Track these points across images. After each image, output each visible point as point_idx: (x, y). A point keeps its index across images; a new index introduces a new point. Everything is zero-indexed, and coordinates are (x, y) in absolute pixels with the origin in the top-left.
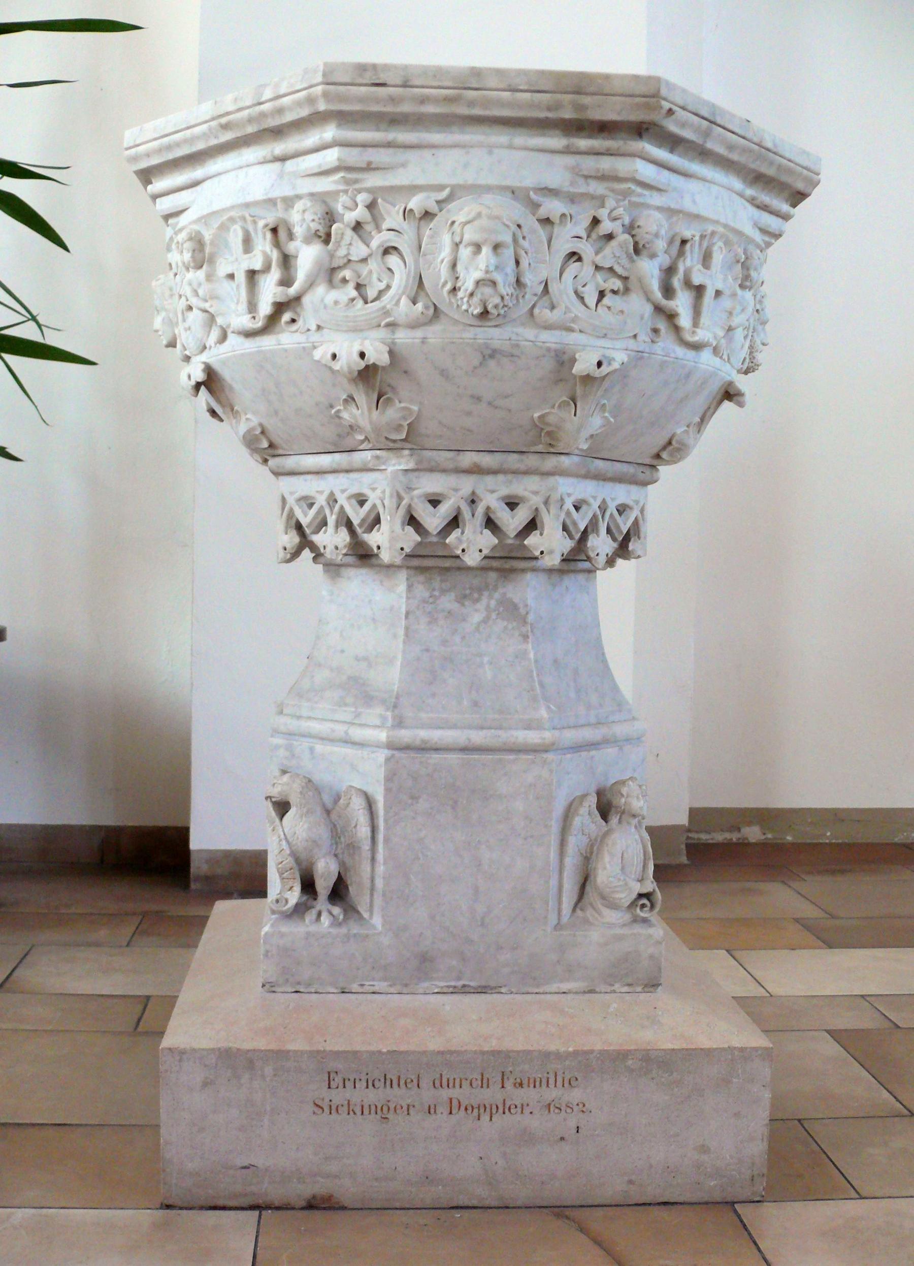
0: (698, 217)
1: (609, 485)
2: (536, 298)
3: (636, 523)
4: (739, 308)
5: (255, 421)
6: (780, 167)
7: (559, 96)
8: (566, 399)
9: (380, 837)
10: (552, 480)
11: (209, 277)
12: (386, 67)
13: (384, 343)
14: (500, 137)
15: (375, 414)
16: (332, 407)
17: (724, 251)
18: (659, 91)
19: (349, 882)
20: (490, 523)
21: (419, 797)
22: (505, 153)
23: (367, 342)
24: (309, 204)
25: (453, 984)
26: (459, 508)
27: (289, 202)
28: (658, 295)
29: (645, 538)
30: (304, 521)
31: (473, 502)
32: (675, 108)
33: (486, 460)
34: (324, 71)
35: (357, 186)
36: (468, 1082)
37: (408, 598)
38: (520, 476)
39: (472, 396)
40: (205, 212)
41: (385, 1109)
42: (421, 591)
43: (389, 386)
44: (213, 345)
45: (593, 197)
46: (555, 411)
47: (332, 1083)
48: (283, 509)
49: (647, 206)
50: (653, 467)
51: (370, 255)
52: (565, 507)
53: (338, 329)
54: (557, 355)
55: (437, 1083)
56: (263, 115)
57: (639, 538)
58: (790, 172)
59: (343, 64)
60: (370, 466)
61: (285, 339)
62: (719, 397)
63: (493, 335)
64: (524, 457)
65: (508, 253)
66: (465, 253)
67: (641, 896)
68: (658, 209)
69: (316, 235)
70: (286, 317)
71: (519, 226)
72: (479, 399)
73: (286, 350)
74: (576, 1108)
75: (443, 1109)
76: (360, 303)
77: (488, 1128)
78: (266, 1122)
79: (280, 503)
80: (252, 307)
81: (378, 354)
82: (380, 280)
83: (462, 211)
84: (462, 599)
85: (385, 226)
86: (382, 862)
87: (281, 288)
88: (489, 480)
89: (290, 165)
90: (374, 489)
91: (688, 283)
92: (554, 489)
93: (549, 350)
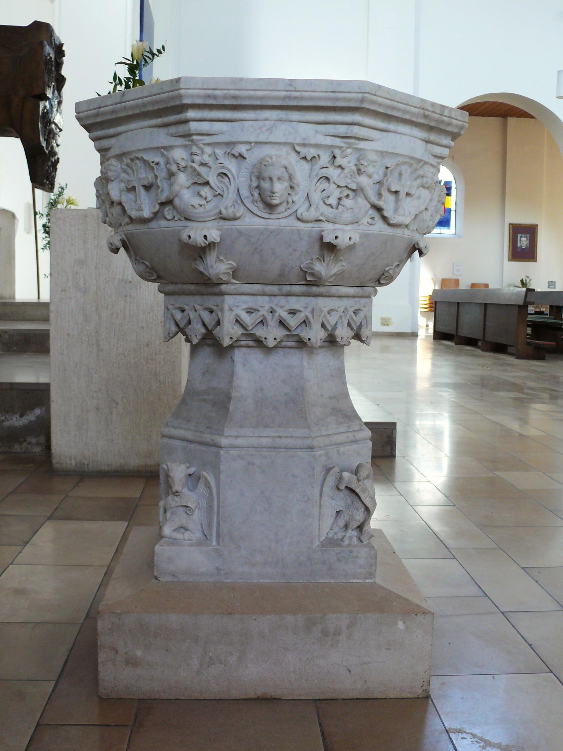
89: (429, 145)
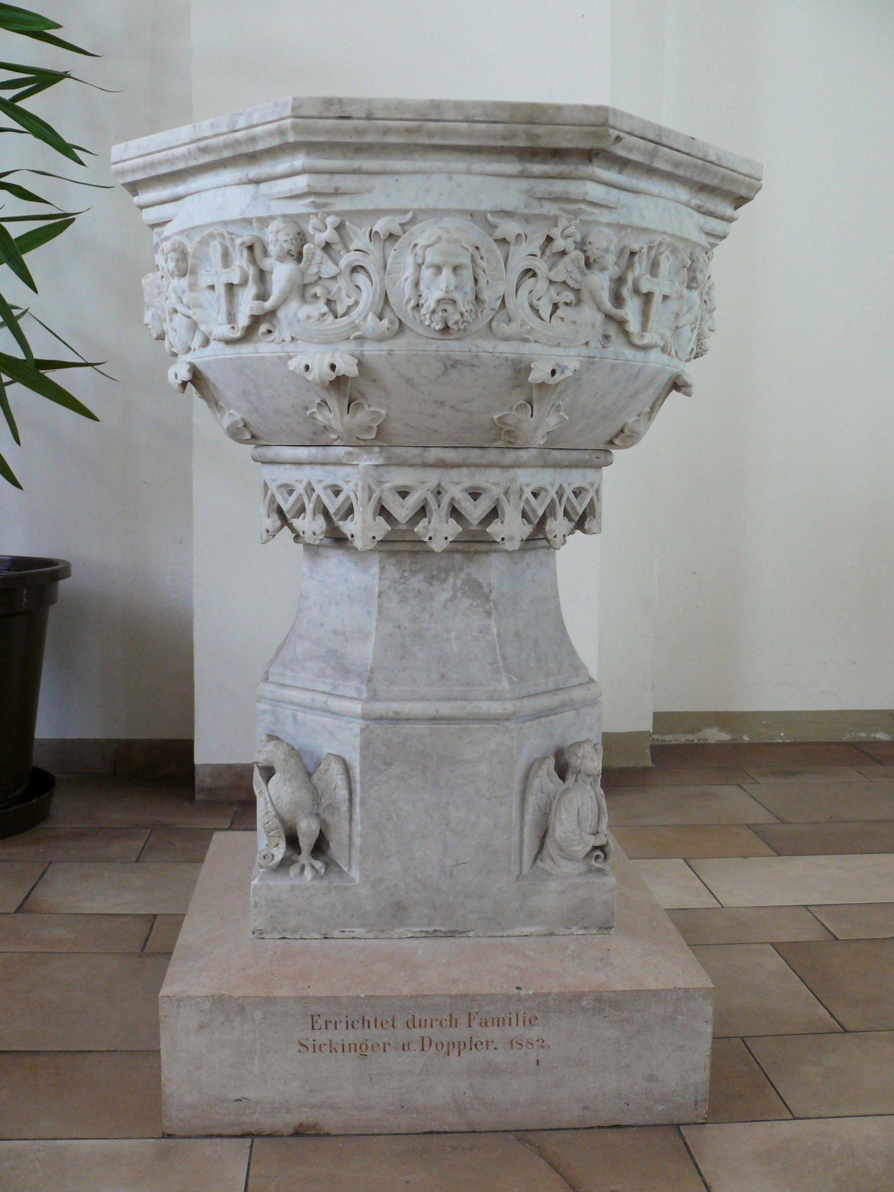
0: (645, 230)
1: (566, 471)
2: (493, 313)
3: (591, 504)
4: (685, 308)
5: (238, 416)
6: (723, 178)
7: (513, 127)
8: (522, 402)
9: (357, 800)
10: (511, 472)
11: (192, 287)
12: (352, 101)
13: (353, 356)
14: (458, 164)
15: (347, 417)
16: (307, 409)
17: (671, 260)
18: (607, 121)
19: (329, 838)
20: (455, 513)
21: (391, 764)
22: (462, 178)
23: (337, 355)
24: (282, 225)
25: (425, 929)
26: (426, 499)
27: (264, 221)
28: (608, 305)
29: (600, 516)
30: (285, 507)
31: (439, 493)
32: (622, 135)
33: (451, 455)
34: (293, 105)
35: (326, 210)
36: (438, 1022)
37: (380, 579)
38: (482, 469)
39: (436, 401)
40: (187, 226)
41: (364, 1047)
42: (392, 572)
43: (359, 392)
44: (197, 348)
45: (546, 217)
46: (514, 413)
47: (315, 1025)
48: (266, 494)
49: (596, 223)
50: (606, 451)
51: (340, 273)
52: (524, 497)
53: (310, 340)
54: (514, 364)
55: (411, 1025)
56: (237, 142)
57: (594, 517)
58: (733, 181)
59: (311, 98)
60: (344, 461)
61: (263, 348)
62: (667, 388)
63: (453, 347)
64: (485, 452)
65: (467, 274)
66: (427, 273)
67: (595, 848)
68: (609, 225)
69: (289, 253)
70: (263, 328)
71: (477, 248)
72: (442, 403)
73: (263, 358)
74: (535, 1044)
75: (416, 1047)
76: (330, 318)
77: (456, 1062)
78: (256, 1058)
79: (263, 489)
80: (231, 318)
81: (347, 367)
82: (348, 296)
83: (424, 234)
84: (430, 580)
85: (352, 247)
86: (359, 821)
87: (257, 302)
88: (454, 473)
90: (348, 482)
91: (636, 291)
92: (513, 480)
93: (506, 359)
